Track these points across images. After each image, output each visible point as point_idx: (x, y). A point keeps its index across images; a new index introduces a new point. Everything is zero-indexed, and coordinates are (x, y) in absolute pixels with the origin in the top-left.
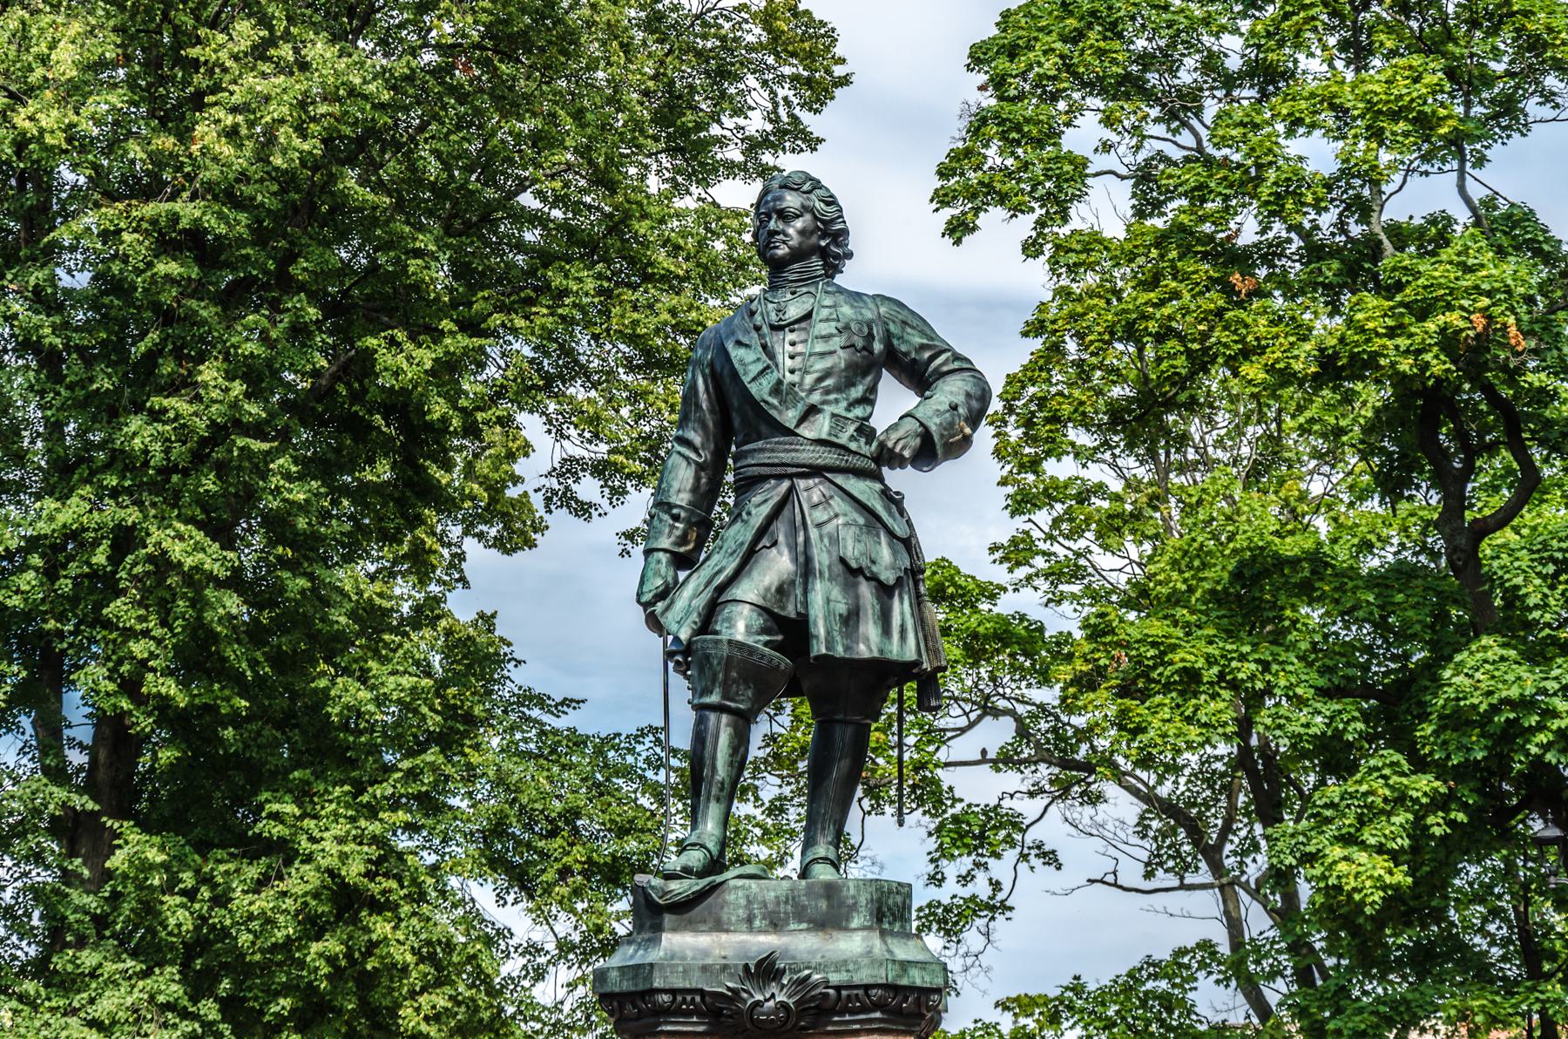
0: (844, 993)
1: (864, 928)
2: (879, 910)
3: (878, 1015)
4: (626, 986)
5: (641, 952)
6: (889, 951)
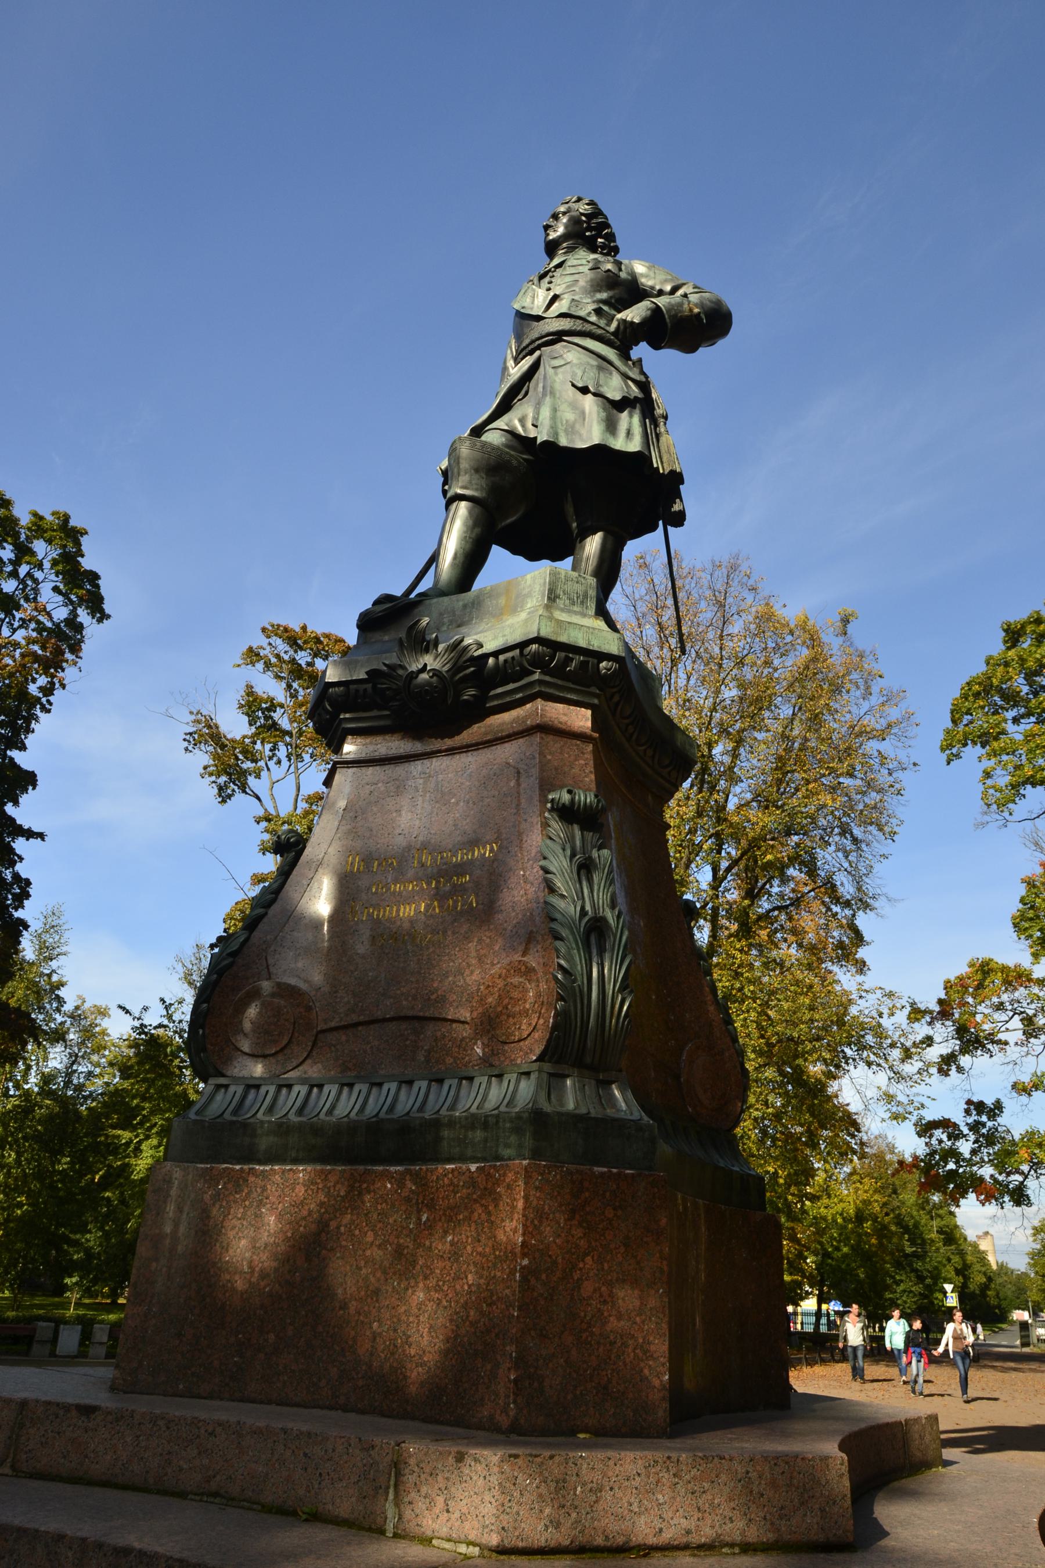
2: (551, 591)
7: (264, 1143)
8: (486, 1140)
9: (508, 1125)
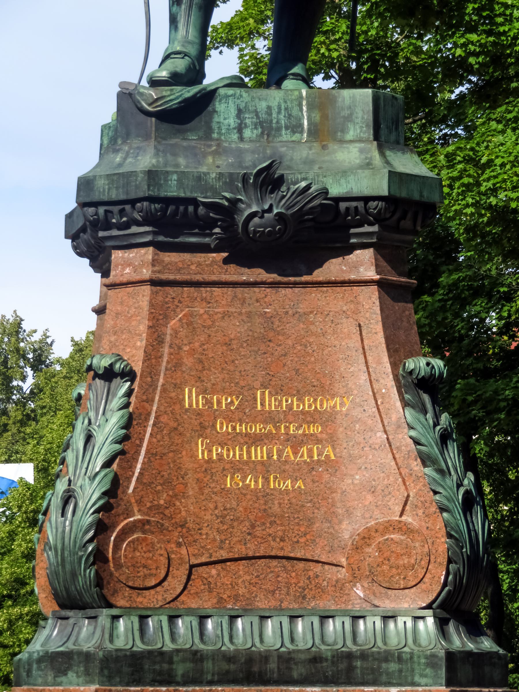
0: (343, 206)
1: (361, 141)
3: (375, 228)
4: (114, 196)
5: (129, 160)
6: (388, 163)
7: (180, 669)
8: (400, 671)
9: (423, 661)
